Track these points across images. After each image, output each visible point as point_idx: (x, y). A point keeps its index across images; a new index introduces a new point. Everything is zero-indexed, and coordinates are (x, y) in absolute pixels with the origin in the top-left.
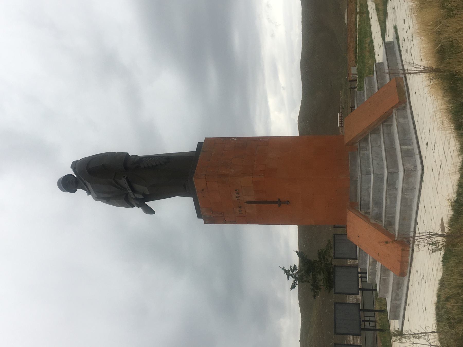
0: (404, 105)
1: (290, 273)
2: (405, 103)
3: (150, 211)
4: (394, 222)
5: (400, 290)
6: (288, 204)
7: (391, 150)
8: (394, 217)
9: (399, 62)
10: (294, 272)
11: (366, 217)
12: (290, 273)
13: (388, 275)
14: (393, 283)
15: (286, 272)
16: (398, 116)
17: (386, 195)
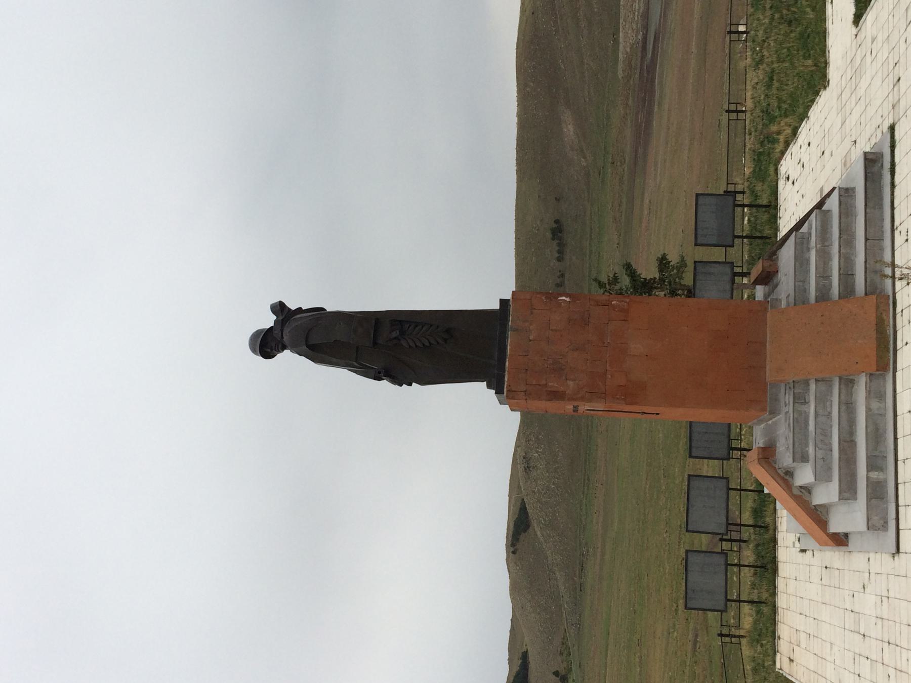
9: (887, 243)
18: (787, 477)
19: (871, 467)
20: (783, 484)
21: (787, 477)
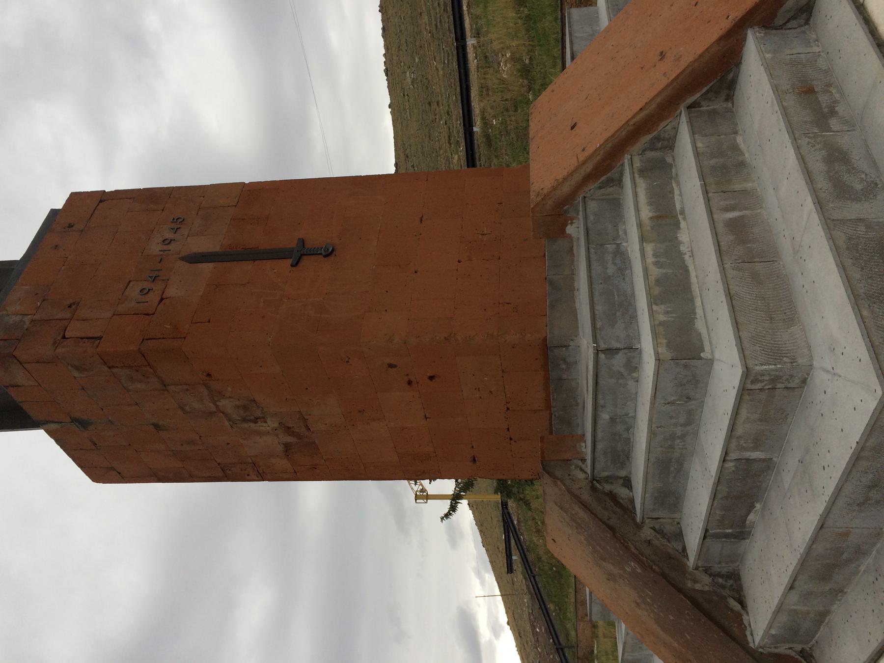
5: (834, 123)
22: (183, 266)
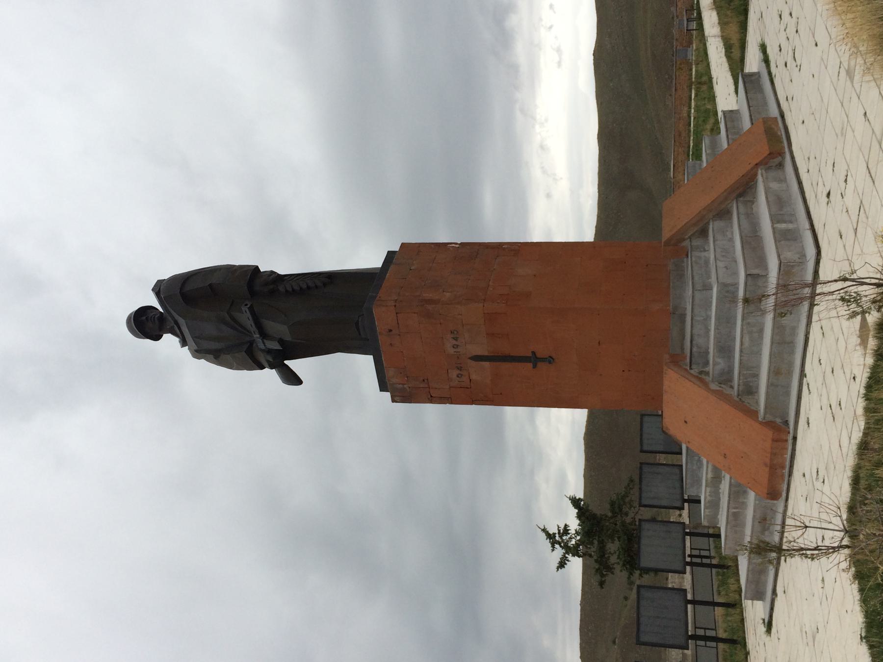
0: (780, 158)
1: (557, 538)
2: (781, 154)
3: (292, 379)
4: (757, 387)
5: (767, 533)
6: (550, 363)
7: (753, 243)
8: (756, 376)
10: (564, 538)
11: (701, 379)
12: (557, 538)
13: (743, 505)
14: (754, 516)
15: (550, 536)
16: (767, 178)
17: (742, 325)
18: (703, 376)
19: (775, 219)
20: (698, 383)
21: (703, 376)
22: (473, 363)
